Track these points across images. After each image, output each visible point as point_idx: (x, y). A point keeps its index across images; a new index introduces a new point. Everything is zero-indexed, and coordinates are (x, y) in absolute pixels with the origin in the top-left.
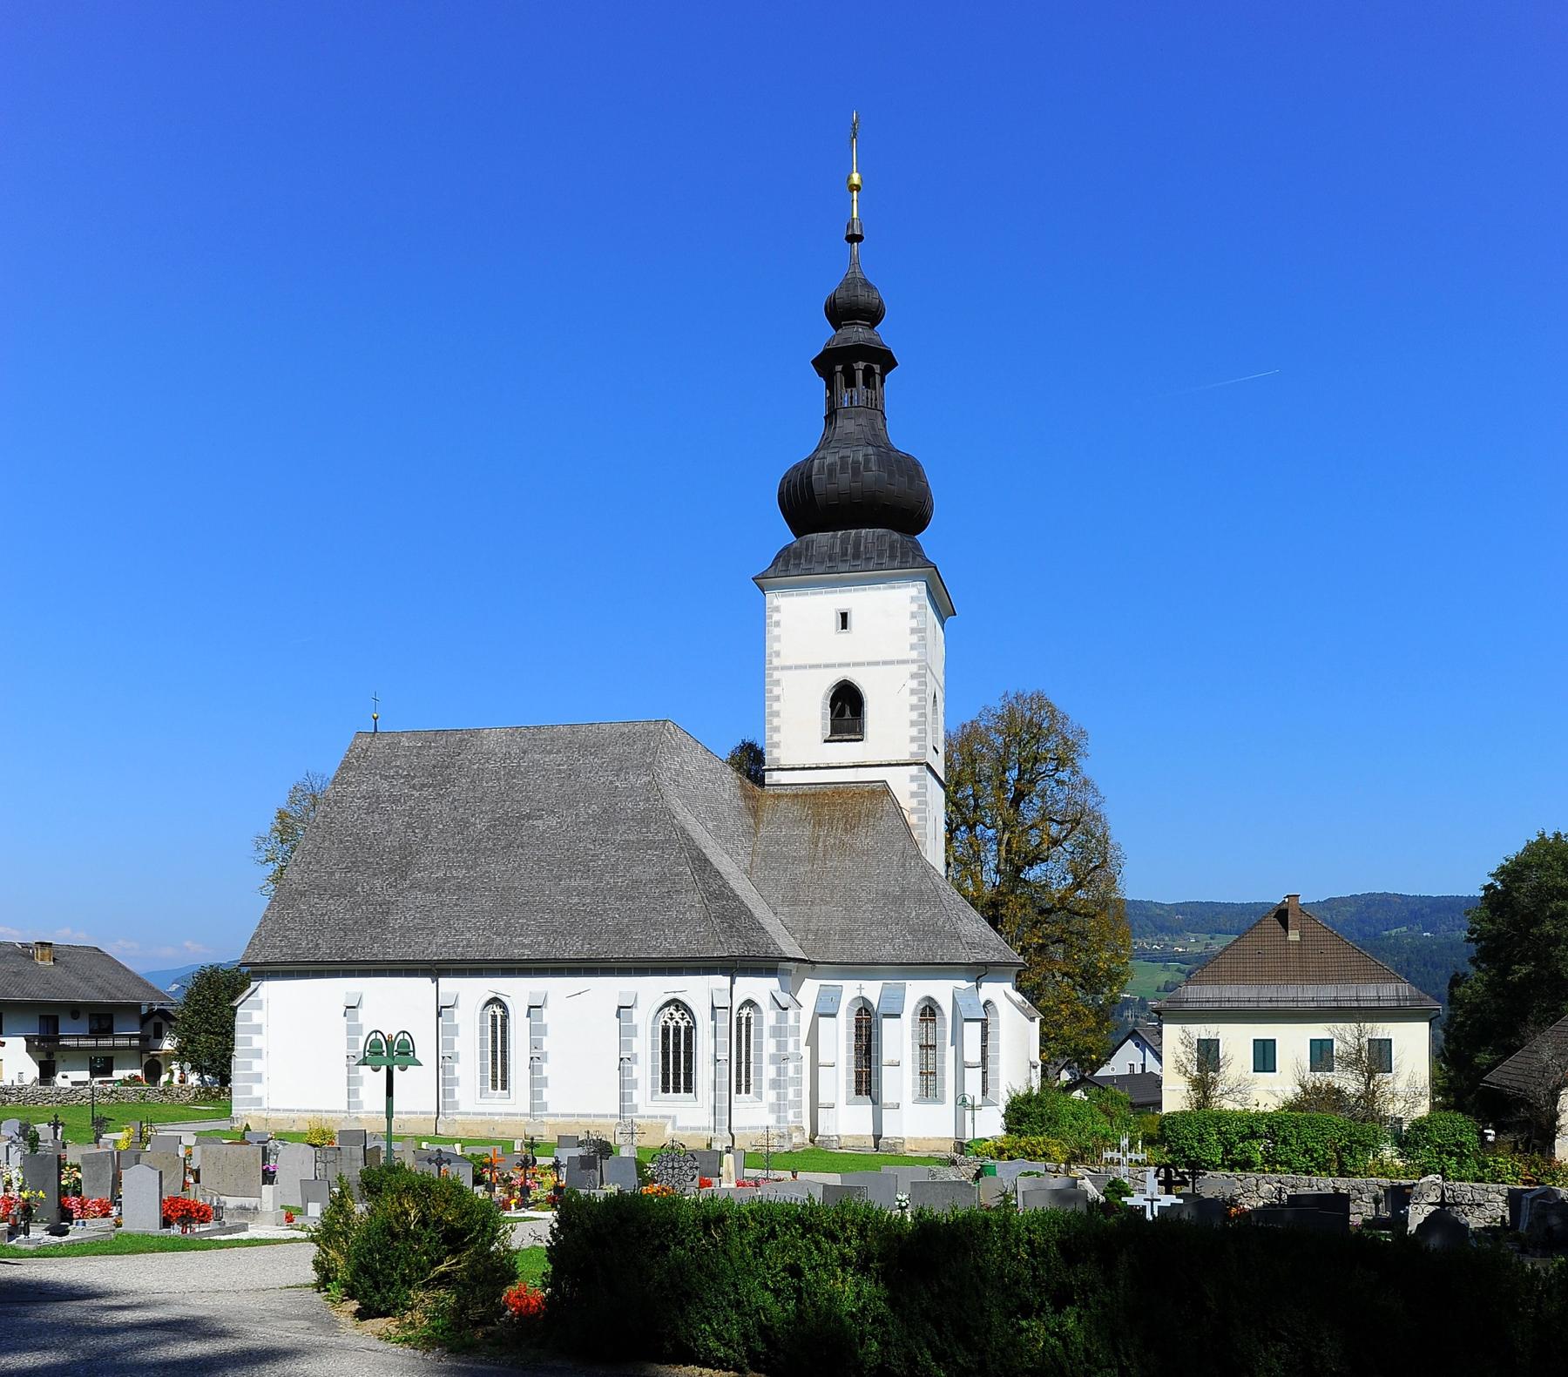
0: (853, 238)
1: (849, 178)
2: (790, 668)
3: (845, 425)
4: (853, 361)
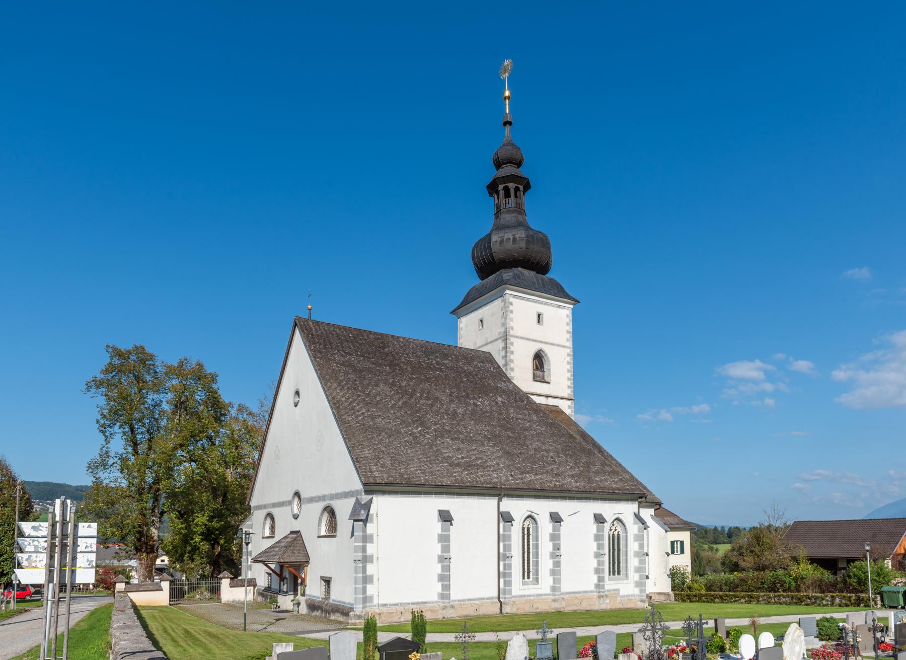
0: (507, 123)
1: (504, 93)
2: (517, 337)
3: (507, 218)
4: (508, 183)
